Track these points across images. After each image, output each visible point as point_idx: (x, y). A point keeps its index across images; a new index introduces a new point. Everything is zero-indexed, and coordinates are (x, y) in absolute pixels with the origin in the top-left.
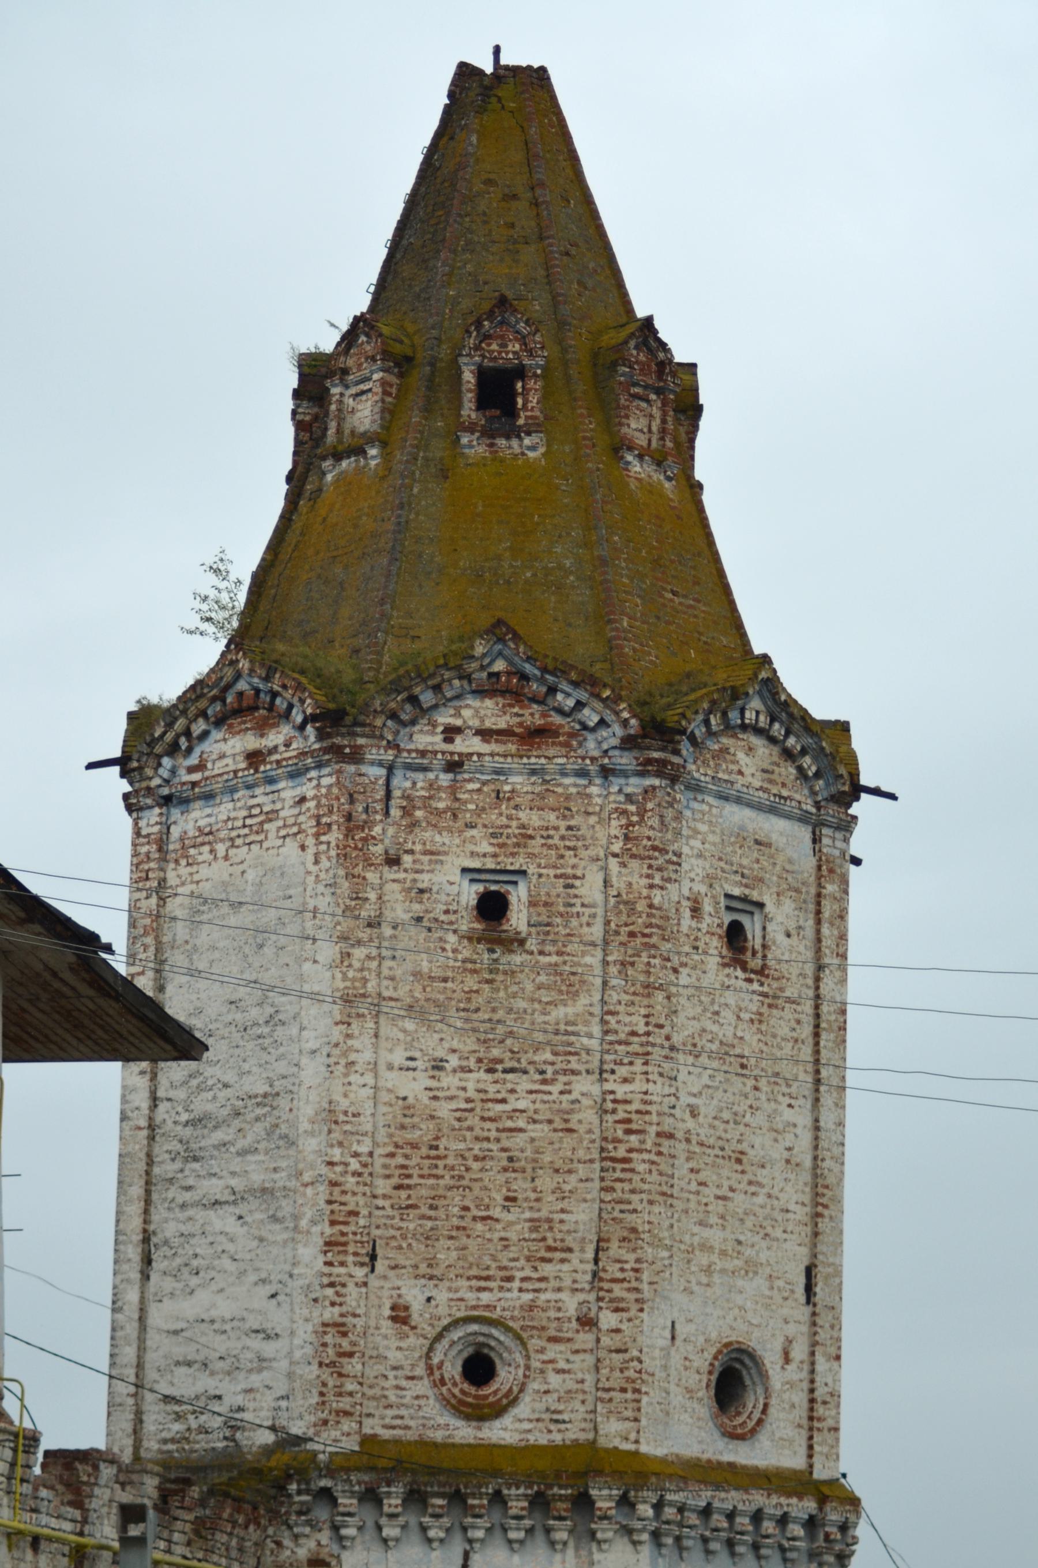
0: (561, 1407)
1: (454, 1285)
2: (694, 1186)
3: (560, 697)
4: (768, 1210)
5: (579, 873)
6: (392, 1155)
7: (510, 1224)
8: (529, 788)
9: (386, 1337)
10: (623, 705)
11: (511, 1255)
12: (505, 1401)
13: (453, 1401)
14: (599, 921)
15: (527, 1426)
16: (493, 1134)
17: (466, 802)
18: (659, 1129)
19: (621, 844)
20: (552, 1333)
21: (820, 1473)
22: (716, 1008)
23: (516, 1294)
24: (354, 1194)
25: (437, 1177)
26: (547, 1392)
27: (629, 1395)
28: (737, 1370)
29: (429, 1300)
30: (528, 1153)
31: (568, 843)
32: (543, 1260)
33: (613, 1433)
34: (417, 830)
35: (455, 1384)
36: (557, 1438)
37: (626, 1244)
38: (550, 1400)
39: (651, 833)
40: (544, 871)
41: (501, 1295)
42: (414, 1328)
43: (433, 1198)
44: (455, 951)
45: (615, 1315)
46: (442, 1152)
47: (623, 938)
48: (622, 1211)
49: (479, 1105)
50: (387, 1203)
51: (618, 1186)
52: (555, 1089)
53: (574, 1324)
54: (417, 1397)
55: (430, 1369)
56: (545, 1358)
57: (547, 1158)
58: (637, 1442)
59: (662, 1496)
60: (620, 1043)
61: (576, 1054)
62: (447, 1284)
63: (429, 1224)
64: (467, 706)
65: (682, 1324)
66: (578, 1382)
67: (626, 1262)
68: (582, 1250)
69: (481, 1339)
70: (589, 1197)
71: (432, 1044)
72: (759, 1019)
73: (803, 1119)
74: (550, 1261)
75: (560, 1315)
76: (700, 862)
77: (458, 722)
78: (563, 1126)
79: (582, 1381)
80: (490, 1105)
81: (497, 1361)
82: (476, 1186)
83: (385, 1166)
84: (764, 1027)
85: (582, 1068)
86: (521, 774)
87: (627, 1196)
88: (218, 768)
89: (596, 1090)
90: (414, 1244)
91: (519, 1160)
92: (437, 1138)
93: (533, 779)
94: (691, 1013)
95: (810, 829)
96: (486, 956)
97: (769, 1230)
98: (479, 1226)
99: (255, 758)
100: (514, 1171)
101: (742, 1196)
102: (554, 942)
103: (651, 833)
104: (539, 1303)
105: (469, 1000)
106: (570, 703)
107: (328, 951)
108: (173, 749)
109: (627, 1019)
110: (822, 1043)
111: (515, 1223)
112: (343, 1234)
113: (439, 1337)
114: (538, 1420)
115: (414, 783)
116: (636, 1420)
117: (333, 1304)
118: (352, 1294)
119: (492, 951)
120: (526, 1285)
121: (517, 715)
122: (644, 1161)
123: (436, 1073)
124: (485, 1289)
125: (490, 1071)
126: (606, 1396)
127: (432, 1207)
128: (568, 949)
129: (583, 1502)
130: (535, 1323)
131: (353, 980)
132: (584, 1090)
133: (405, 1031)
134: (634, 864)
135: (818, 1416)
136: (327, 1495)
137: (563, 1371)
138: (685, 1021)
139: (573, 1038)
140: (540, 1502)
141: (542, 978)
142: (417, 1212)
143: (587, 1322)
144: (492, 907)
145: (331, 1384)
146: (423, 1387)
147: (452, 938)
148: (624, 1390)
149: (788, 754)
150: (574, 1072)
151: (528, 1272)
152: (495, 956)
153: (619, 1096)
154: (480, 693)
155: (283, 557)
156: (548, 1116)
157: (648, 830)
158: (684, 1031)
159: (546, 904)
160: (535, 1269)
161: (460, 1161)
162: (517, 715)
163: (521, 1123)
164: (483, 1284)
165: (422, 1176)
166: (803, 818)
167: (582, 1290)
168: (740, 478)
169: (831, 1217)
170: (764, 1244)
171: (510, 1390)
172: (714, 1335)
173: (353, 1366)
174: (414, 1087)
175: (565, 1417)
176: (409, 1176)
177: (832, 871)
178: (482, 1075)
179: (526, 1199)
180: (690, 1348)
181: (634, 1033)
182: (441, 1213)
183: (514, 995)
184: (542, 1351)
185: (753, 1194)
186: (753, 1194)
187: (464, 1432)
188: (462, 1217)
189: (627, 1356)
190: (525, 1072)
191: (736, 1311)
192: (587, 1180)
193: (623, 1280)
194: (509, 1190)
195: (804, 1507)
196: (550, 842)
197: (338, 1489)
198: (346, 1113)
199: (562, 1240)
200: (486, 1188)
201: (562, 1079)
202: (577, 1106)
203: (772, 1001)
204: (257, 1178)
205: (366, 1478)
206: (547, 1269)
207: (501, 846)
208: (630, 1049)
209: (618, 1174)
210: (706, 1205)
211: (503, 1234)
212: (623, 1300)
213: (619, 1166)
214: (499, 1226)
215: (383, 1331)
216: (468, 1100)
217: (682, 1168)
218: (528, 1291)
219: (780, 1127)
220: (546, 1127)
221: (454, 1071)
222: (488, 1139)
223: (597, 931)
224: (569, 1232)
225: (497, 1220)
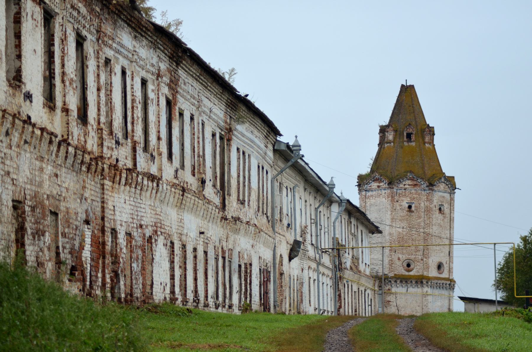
21: (451, 278)
33: (425, 274)
71: (402, 225)
72: (443, 220)
73: (448, 232)
88: (373, 187)
99: (379, 187)
107: (389, 213)
108: (367, 184)
118: (393, 256)
129: (422, 282)
135: (450, 271)
136: (390, 281)
140: (416, 282)
143: (422, 260)
144: (410, 207)
146: (402, 268)
149: (447, 185)
154: (408, 180)
155: (380, 156)
157: (430, 198)
158: (434, 222)
166: (449, 193)
168: (440, 143)
173: (393, 265)
174: (400, 230)
177: (452, 199)
187: (407, 273)
195: (449, 282)
197: (392, 280)
203: (445, 217)
204: (380, 241)
206: (417, 253)
217: (434, 240)
223: (423, 210)
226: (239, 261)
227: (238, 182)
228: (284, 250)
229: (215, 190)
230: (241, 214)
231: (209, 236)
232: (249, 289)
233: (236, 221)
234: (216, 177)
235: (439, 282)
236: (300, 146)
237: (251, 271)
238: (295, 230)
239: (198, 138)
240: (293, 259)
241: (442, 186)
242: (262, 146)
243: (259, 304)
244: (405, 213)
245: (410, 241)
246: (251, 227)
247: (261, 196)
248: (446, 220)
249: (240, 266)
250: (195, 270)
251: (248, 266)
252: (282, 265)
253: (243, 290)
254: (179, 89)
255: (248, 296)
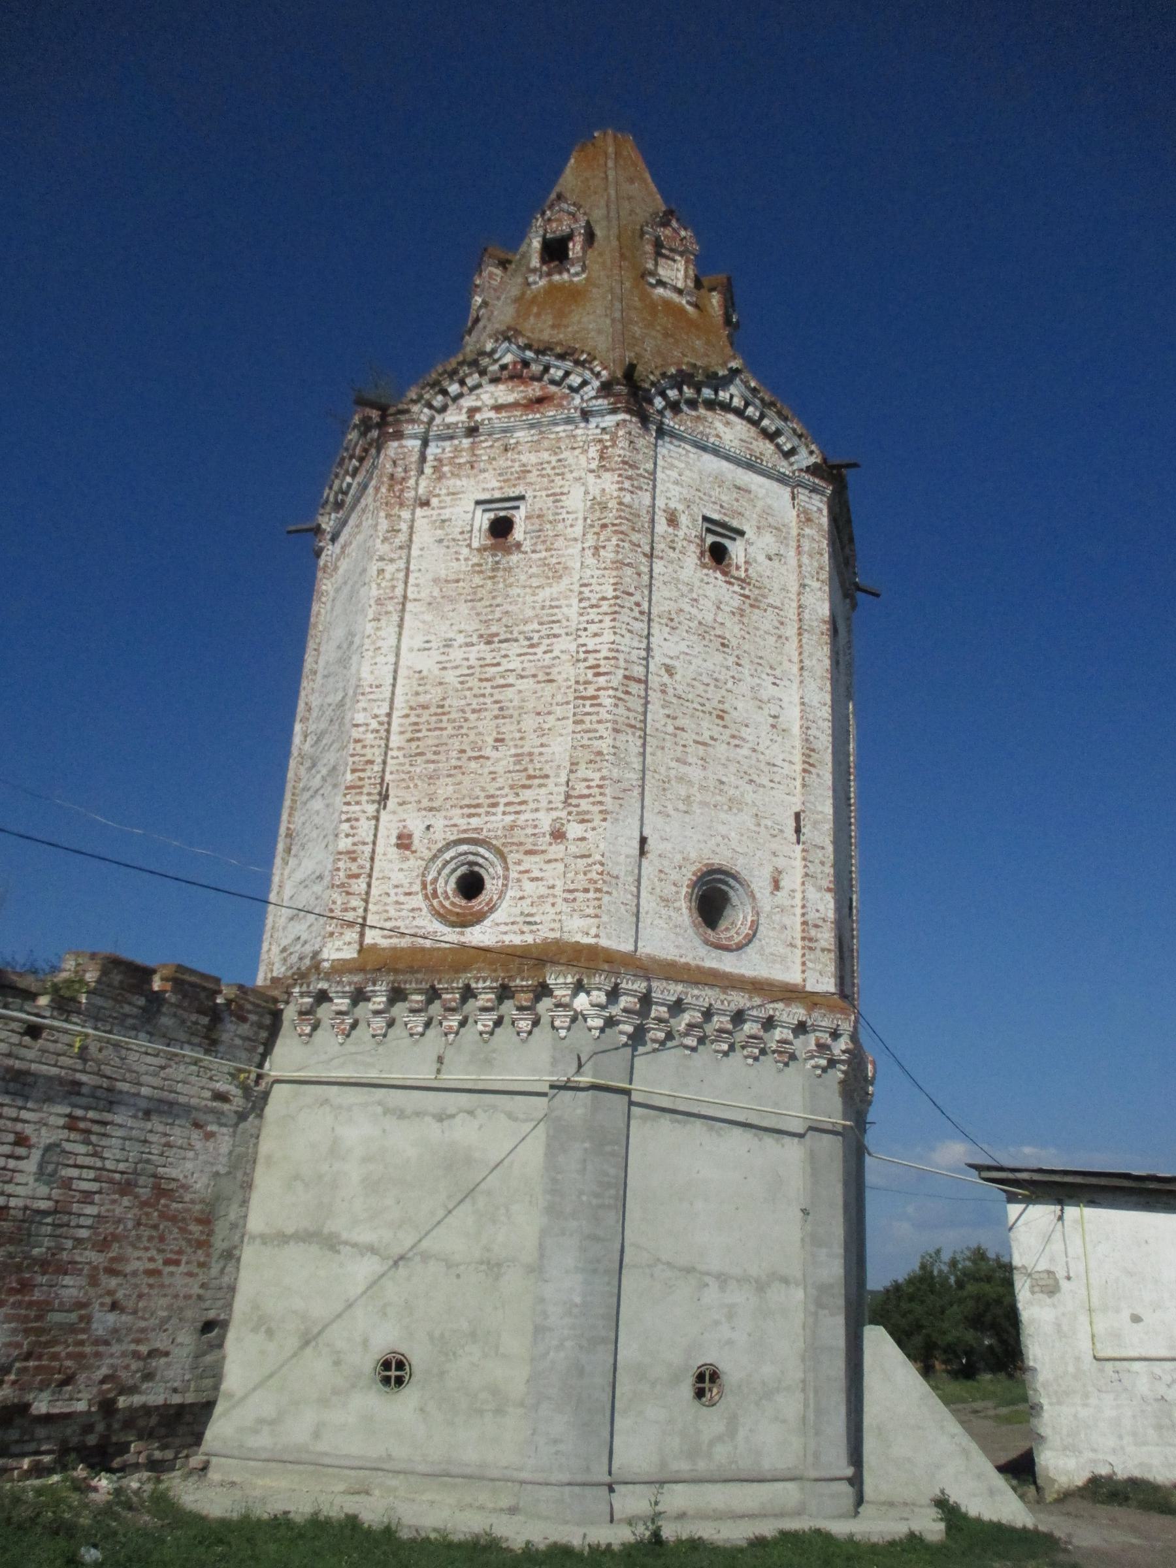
0: (534, 910)
1: (449, 814)
2: (670, 729)
3: (552, 371)
4: (753, 762)
5: (565, 490)
6: (407, 716)
7: (498, 760)
8: (530, 439)
9: (391, 861)
10: (596, 363)
11: (498, 785)
12: (486, 908)
13: (442, 911)
14: (580, 522)
15: (504, 928)
16: (489, 691)
17: (481, 455)
18: (627, 673)
19: (597, 462)
20: (530, 847)
22: (694, 596)
23: (500, 817)
24: (372, 746)
25: (441, 729)
26: (522, 898)
27: (591, 895)
28: (723, 890)
29: (428, 827)
30: (516, 703)
31: (557, 471)
32: (524, 787)
34: (444, 481)
35: (447, 898)
36: (530, 939)
37: (592, 766)
38: (525, 906)
39: (621, 452)
40: (538, 494)
41: (487, 819)
42: (415, 852)
43: (437, 746)
44: (466, 559)
45: (580, 825)
46: (447, 709)
47: (596, 530)
48: (590, 739)
49: (478, 670)
50: (400, 754)
51: (587, 719)
52: (539, 651)
53: (548, 838)
54: (413, 910)
55: (424, 886)
56: (522, 868)
57: (530, 706)
58: (597, 936)
59: (617, 985)
60: (592, 606)
61: (558, 621)
62: (444, 813)
63: (432, 766)
64: (486, 392)
66: (549, 888)
67: (592, 780)
68: (557, 776)
69: (471, 858)
70: (564, 732)
72: (742, 612)
74: (529, 787)
75: (536, 831)
76: (678, 488)
77: (479, 404)
78: (547, 678)
79: (553, 887)
80: (487, 669)
81: (486, 877)
82: (472, 733)
83: (401, 725)
84: (745, 620)
85: (562, 631)
86: (523, 429)
87: (595, 726)
89: (573, 647)
90: (419, 783)
91: (508, 708)
92: (444, 699)
93: (533, 432)
94: (667, 594)
95: (789, 489)
96: (490, 559)
97: (755, 777)
98: (473, 765)
100: (504, 717)
101: (724, 746)
102: (544, 542)
103: (621, 452)
104: (519, 823)
105: (475, 593)
106: (560, 373)
109: (598, 588)
110: (804, 641)
111: (502, 760)
112: (361, 779)
113: (435, 857)
114: (513, 923)
115: (444, 450)
116: (596, 916)
117: (347, 836)
119: (494, 555)
120: (508, 809)
121: (522, 392)
122: (609, 696)
123: (446, 650)
124: (473, 815)
125: (489, 643)
126: (571, 896)
127: (435, 753)
128: (555, 546)
130: (515, 840)
131: (386, 587)
132: (564, 648)
133: (424, 622)
134: (607, 476)
137: (537, 879)
138: (661, 600)
139: (556, 610)
141: (534, 570)
142: (424, 758)
143: (558, 835)
144: (501, 528)
145: (339, 902)
146: (418, 901)
147: (465, 551)
148: (586, 891)
150: (555, 636)
151: (511, 798)
152: (497, 559)
153: (590, 648)
154: (495, 380)
156: (533, 671)
159: (539, 516)
160: (517, 794)
161: (461, 714)
162: (522, 392)
163: (511, 680)
164: (472, 811)
165: (429, 730)
167: (556, 809)
169: (818, 775)
170: (750, 788)
171: (491, 900)
172: (693, 855)
175: (537, 919)
176: (419, 731)
178: (482, 647)
179: (513, 739)
180: (666, 863)
181: (604, 599)
182: (442, 757)
183: (511, 585)
184: (519, 863)
185: (736, 746)
186: (736, 746)
187: (450, 936)
188: (459, 759)
189: (590, 861)
190: (516, 640)
191: (719, 838)
192: (563, 718)
193: (589, 796)
194: (498, 733)
196: (544, 472)
198: (371, 686)
199: (541, 769)
200: (480, 734)
201: (546, 641)
202: (557, 661)
205: (356, 979)
206: (526, 794)
207: (504, 481)
208: (600, 610)
209: (588, 709)
210: (684, 746)
211: (492, 769)
212: (587, 812)
213: (588, 703)
214: (489, 763)
215: (389, 856)
216: (470, 667)
218: (510, 813)
219: (765, 698)
220: (531, 680)
221: (461, 647)
222: (484, 695)
223: (578, 530)
224: (547, 762)
225: (488, 758)
235: (707, 996)
245: (487, 726)
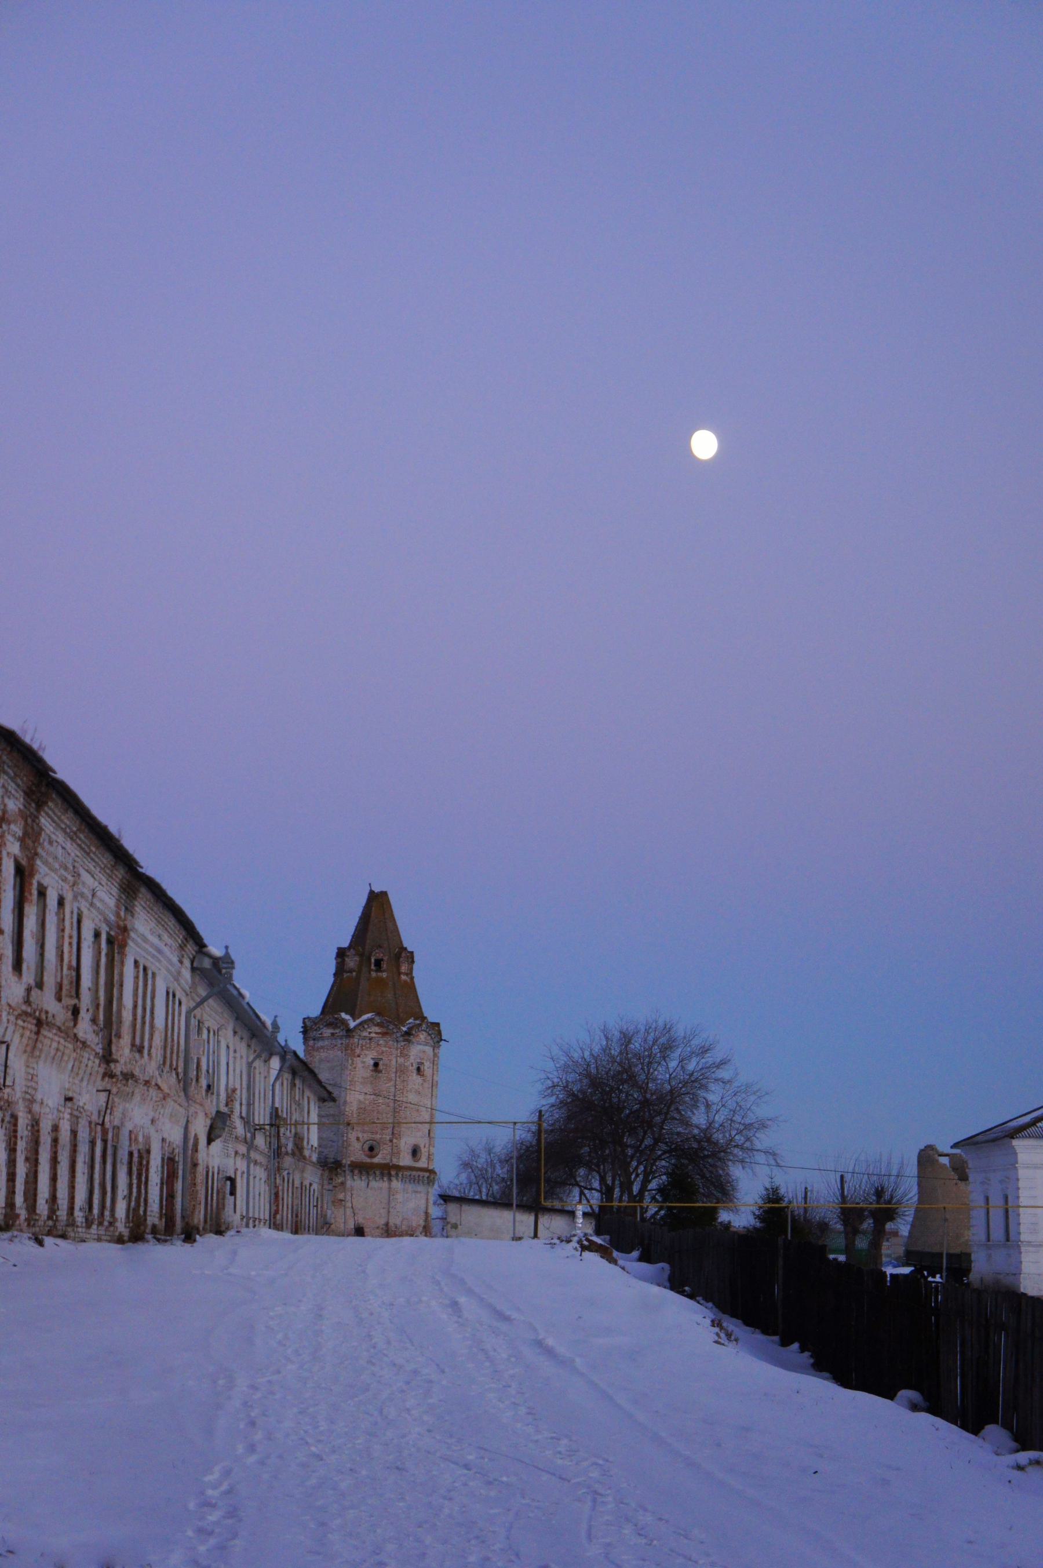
21: (431, 1168)
33: (395, 1161)
65: (406, 1143)
99: (333, 1034)
129: (390, 1175)
143: (391, 1141)
157: (405, 1052)
174: (361, 1097)
177: (435, 1055)
187: (368, 1160)
195: (427, 1174)
226: (130, 1145)
227: (135, 1015)
228: (200, 1127)
229: (95, 1028)
230: (137, 1069)
231: (81, 1104)
232: (143, 1191)
233: (127, 1080)
234: (98, 1006)
235: (414, 1173)
236: (232, 962)
237: (148, 1162)
238: (218, 1095)
239: (71, 937)
240: (213, 1140)
241: (423, 1036)
242: (175, 960)
243: (157, 1215)
244: (368, 1073)
246: (151, 1090)
247: (169, 1040)
248: (426, 1085)
249: (131, 1154)
250: (54, 1161)
251: (145, 1156)
252: (197, 1151)
253: (134, 1194)
254: (40, 850)
255: (142, 1204)
